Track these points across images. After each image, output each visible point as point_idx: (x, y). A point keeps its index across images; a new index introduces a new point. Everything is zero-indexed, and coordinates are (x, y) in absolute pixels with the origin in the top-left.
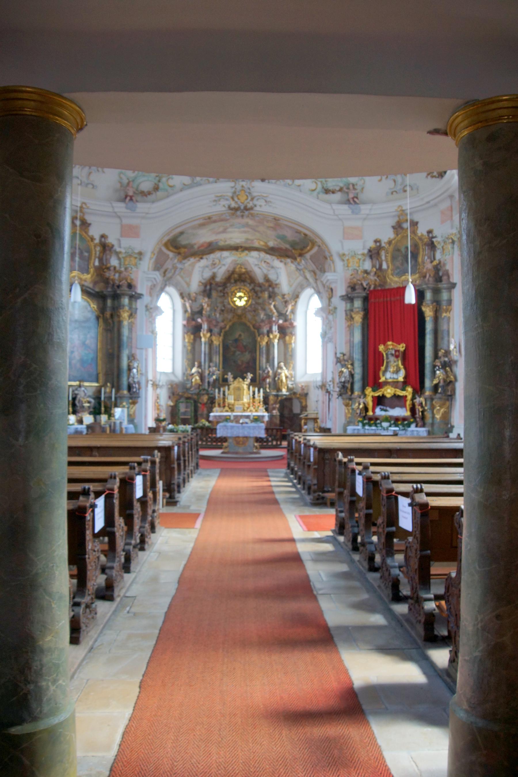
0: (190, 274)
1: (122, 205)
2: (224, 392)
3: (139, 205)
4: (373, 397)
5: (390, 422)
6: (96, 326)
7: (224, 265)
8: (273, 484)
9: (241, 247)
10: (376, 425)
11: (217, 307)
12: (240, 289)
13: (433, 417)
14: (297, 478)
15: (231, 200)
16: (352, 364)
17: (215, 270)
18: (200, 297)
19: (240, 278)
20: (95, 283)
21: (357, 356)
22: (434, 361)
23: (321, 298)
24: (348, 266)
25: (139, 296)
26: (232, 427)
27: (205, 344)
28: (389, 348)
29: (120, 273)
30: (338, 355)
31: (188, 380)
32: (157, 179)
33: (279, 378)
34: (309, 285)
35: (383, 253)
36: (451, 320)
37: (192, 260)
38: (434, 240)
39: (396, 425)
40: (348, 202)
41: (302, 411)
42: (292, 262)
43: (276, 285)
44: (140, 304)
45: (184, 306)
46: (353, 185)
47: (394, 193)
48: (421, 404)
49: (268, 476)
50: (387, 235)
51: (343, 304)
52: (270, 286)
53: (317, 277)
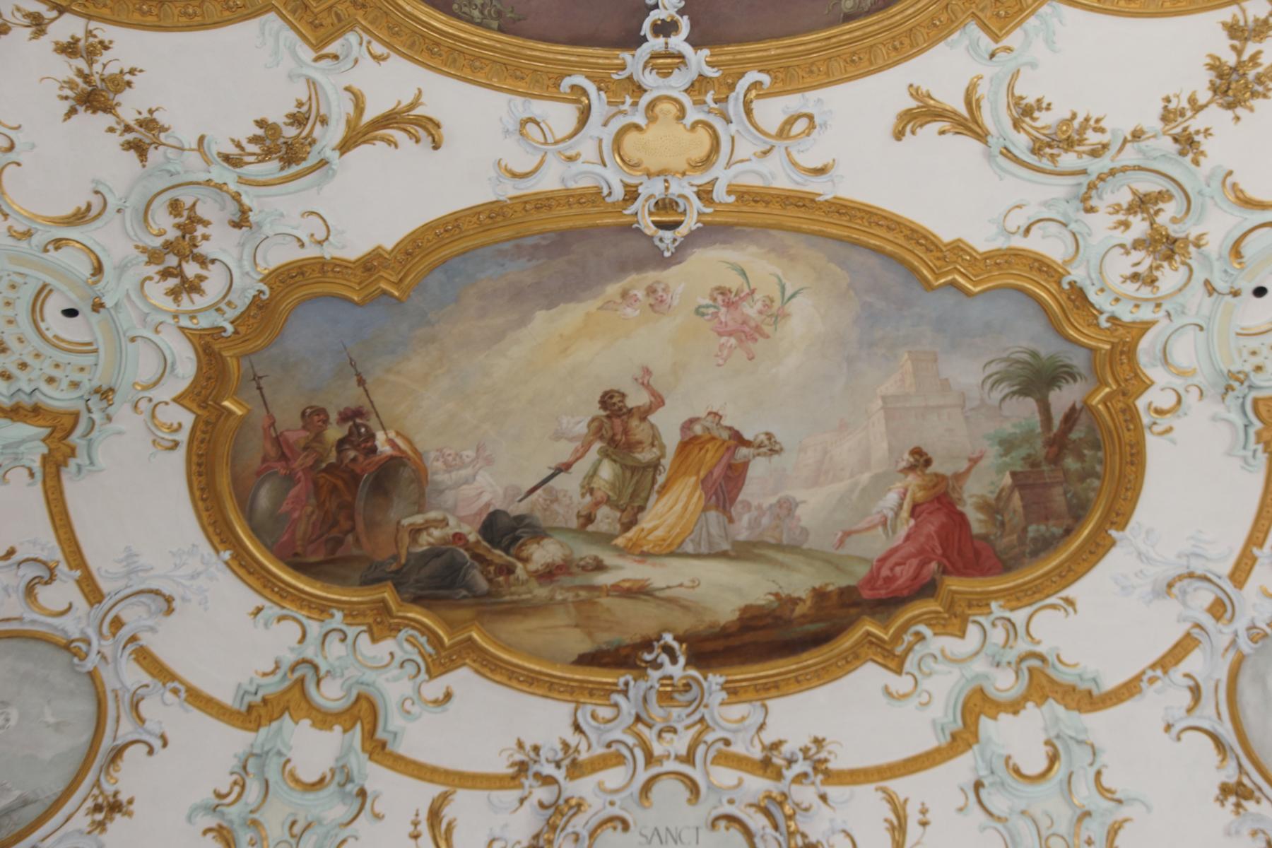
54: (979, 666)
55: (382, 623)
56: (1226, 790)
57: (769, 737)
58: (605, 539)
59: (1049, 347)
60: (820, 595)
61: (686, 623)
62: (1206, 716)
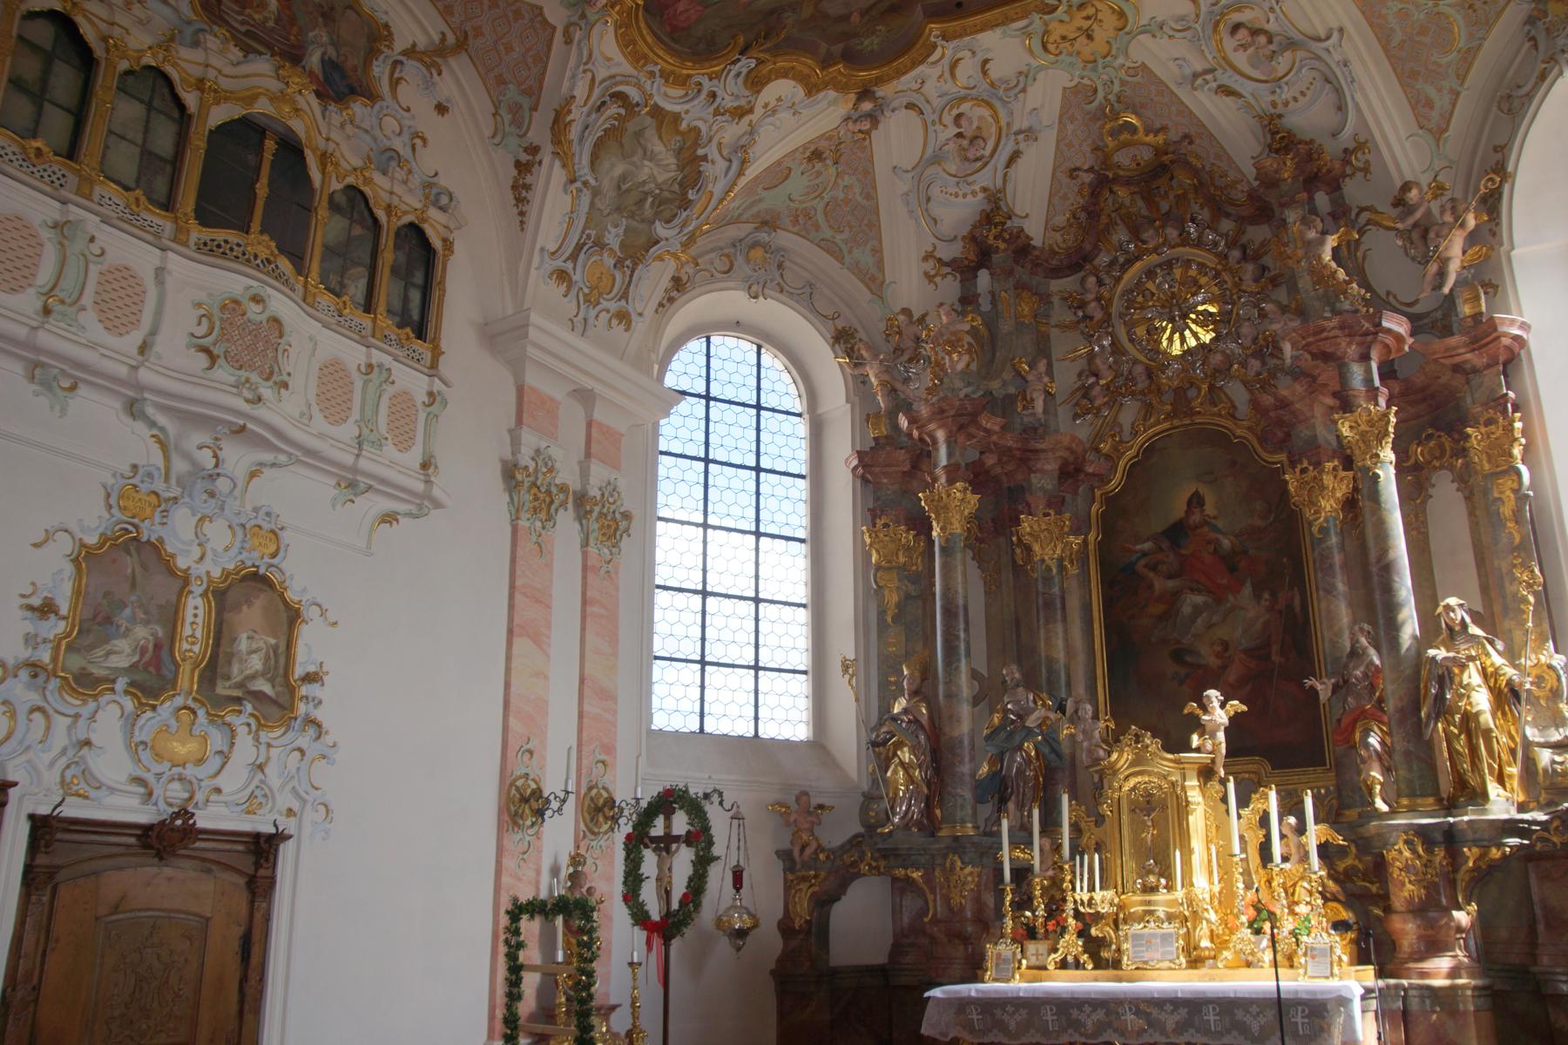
7: (1029, 134)
33: (1442, 709)
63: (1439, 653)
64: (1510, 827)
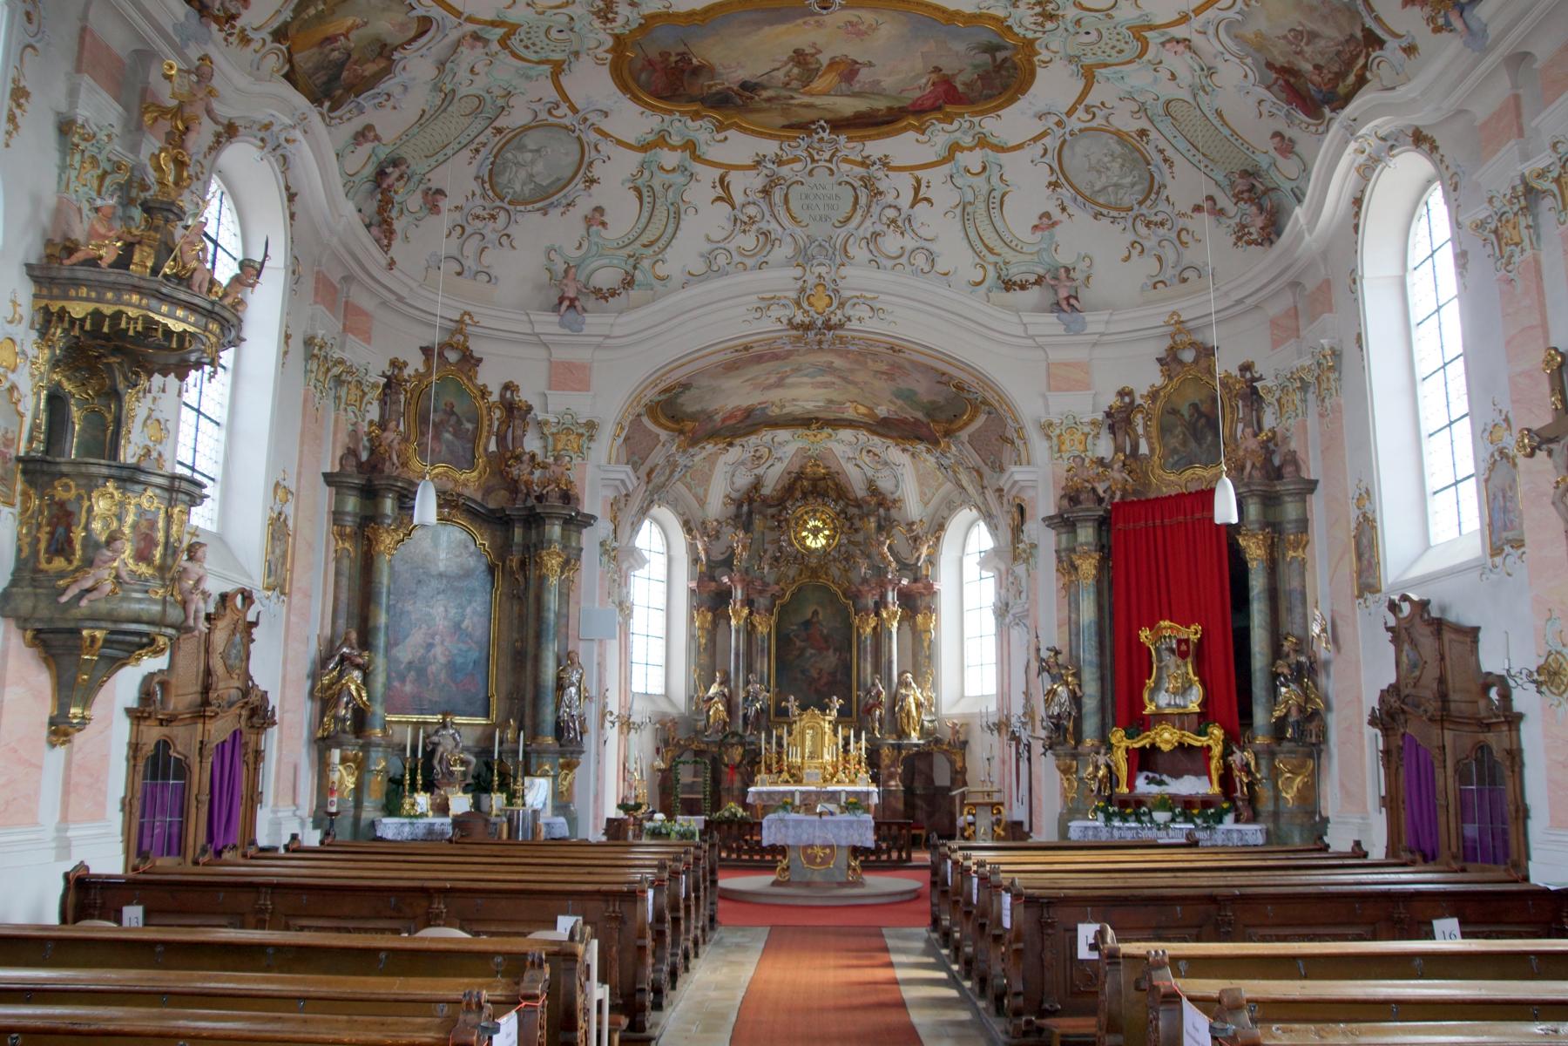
0: (706, 479)
1: (554, 318)
2: (780, 738)
3: (589, 318)
4: (1127, 750)
5: (1171, 810)
6: (488, 587)
7: (780, 459)
8: (900, 974)
9: (817, 419)
10: (1139, 820)
11: (765, 551)
12: (815, 511)
13: (1277, 797)
14: (961, 960)
15: (794, 309)
16: (1077, 675)
17: (760, 471)
18: (728, 531)
19: (814, 487)
20: (487, 491)
21: (1088, 654)
22: (1273, 664)
23: (993, 528)
24: (1060, 451)
25: (588, 520)
26: (799, 823)
27: (738, 631)
28: (1166, 636)
29: (545, 467)
30: (1044, 654)
31: (698, 711)
32: (631, 261)
33: (902, 708)
34: (966, 502)
35: (1139, 419)
36: (1308, 566)
37: (710, 447)
38: (1258, 385)
39: (1189, 819)
40: (1057, 307)
41: (953, 781)
42: (928, 451)
43: (895, 501)
44: (589, 539)
45: (692, 548)
46: (1067, 270)
47: (1160, 286)
48: (1246, 767)
49: (886, 950)
50: (1146, 378)
51: (1052, 533)
52: (880, 504)
53: (985, 483)
54: (958, 134)
55: (696, 116)
56: (1050, 184)
57: (865, 154)
58: (796, 90)
59: (996, 40)
60: (890, 109)
61: (829, 116)
62: (1047, 159)
63: (903, 691)
64: (917, 745)
